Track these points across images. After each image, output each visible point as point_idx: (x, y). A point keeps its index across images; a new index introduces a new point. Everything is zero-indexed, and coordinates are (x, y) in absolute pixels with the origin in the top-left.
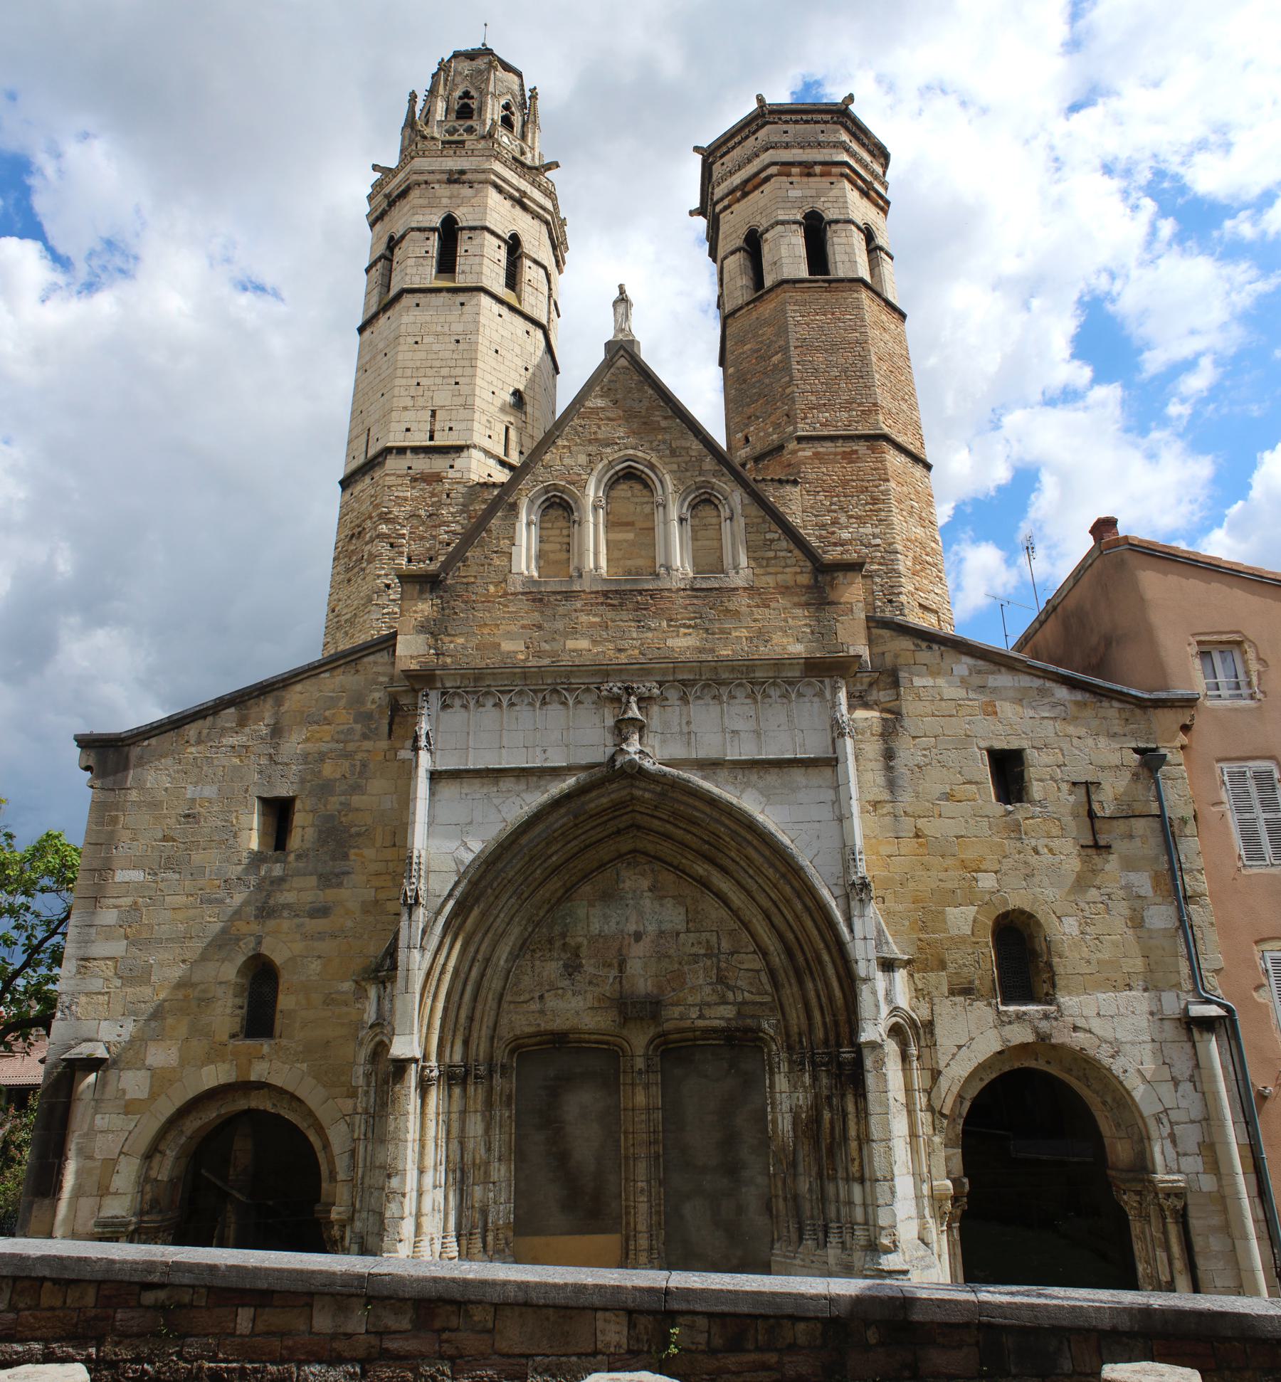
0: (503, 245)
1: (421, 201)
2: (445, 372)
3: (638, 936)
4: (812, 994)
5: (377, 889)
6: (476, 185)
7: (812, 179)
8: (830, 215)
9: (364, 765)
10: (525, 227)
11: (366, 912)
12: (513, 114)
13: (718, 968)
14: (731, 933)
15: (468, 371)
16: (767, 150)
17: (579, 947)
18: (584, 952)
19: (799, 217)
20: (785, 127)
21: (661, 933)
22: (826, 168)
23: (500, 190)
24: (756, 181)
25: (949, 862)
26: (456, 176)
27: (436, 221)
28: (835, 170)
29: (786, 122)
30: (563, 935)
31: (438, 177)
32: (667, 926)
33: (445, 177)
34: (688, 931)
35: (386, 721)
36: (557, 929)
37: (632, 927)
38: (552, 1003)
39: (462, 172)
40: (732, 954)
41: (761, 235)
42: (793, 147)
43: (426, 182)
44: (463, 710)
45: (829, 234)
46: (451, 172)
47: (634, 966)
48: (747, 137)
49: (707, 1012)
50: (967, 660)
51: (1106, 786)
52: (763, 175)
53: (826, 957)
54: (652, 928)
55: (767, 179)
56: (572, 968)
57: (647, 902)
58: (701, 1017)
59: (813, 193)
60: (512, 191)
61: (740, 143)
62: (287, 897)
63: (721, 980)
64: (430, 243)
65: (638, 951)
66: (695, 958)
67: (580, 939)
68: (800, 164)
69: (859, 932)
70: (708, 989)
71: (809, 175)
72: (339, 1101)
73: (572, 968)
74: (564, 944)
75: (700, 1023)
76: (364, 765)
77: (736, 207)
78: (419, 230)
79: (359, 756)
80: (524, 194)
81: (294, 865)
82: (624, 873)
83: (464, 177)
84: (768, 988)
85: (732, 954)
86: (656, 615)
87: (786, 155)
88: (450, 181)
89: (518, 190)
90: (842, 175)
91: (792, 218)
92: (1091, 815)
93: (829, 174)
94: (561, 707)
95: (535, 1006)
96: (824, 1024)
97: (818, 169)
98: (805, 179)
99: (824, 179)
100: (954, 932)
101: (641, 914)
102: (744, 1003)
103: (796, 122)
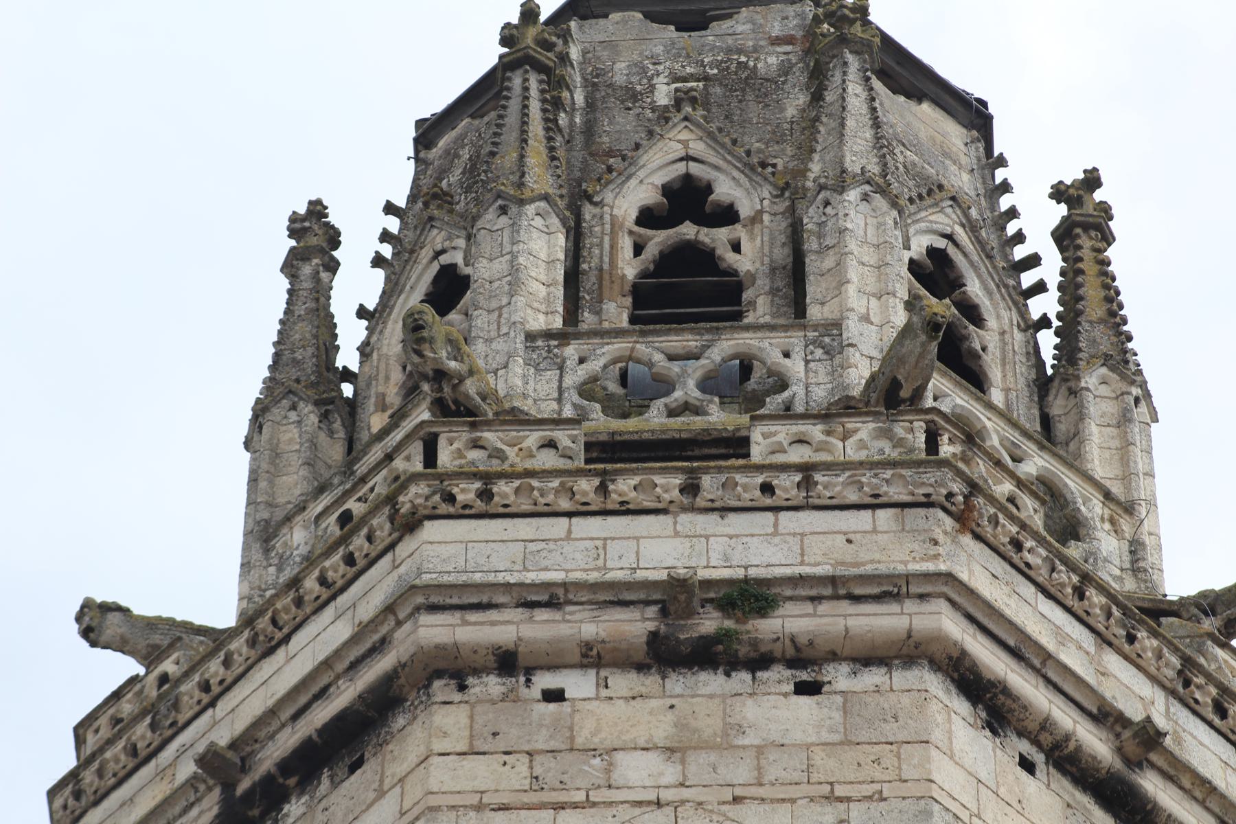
1: (481, 774)
6: (839, 677)
23: (995, 708)
26: (709, 623)
31: (587, 625)
33: (634, 626)
39: (750, 596)
43: (507, 662)
46: (675, 596)
60: (1066, 718)
80: (1146, 741)
83: (767, 627)
88: (666, 656)
89: (1105, 716)
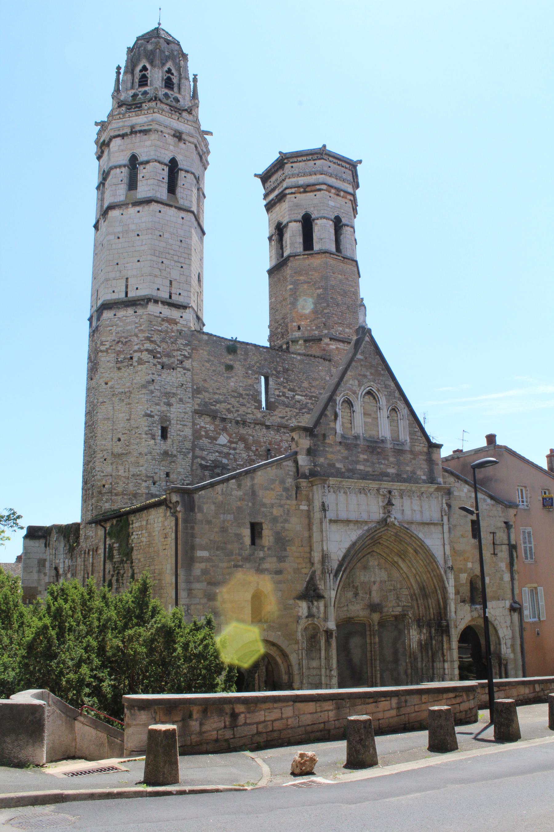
2: (176, 258)
3: (374, 583)
4: (430, 603)
5: (298, 564)
9: (288, 511)
11: (294, 573)
13: (397, 595)
14: (400, 582)
15: (187, 261)
16: (322, 174)
17: (357, 587)
18: (359, 588)
19: (333, 217)
20: (330, 164)
21: (381, 582)
22: (345, 194)
24: (313, 188)
25: (462, 558)
27: (167, 160)
29: (330, 161)
30: (353, 582)
32: (382, 579)
33: (173, 132)
34: (388, 581)
35: (294, 492)
36: (351, 579)
37: (373, 579)
38: (351, 607)
40: (400, 589)
41: (314, 220)
42: (333, 177)
43: (161, 132)
44: (334, 494)
47: (374, 594)
48: (310, 160)
49: (394, 609)
50: (467, 486)
51: (497, 534)
52: (318, 187)
53: (439, 592)
54: (378, 579)
55: (320, 190)
56: (356, 595)
57: (377, 570)
58: (393, 611)
61: (305, 161)
62: (266, 566)
63: (398, 598)
65: (375, 588)
66: (391, 591)
67: (358, 584)
68: (335, 188)
69: (450, 585)
70: (394, 602)
71: (338, 195)
72: (293, 645)
73: (356, 595)
74: (353, 586)
75: (393, 613)
76: (288, 511)
77: (298, 195)
78: (159, 162)
79: (286, 507)
81: (267, 552)
82: (370, 559)
84: (410, 601)
85: (400, 589)
86: (384, 459)
87: (332, 181)
92: (494, 544)
93: (346, 198)
94: (364, 496)
95: (345, 609)
96: (434, 613)
97: (342, 194)
98: (336, 197)
99: (343, 199)
100: (462, 582)
101: (375, 574)
102: (404, 606)
103: (335, 163)
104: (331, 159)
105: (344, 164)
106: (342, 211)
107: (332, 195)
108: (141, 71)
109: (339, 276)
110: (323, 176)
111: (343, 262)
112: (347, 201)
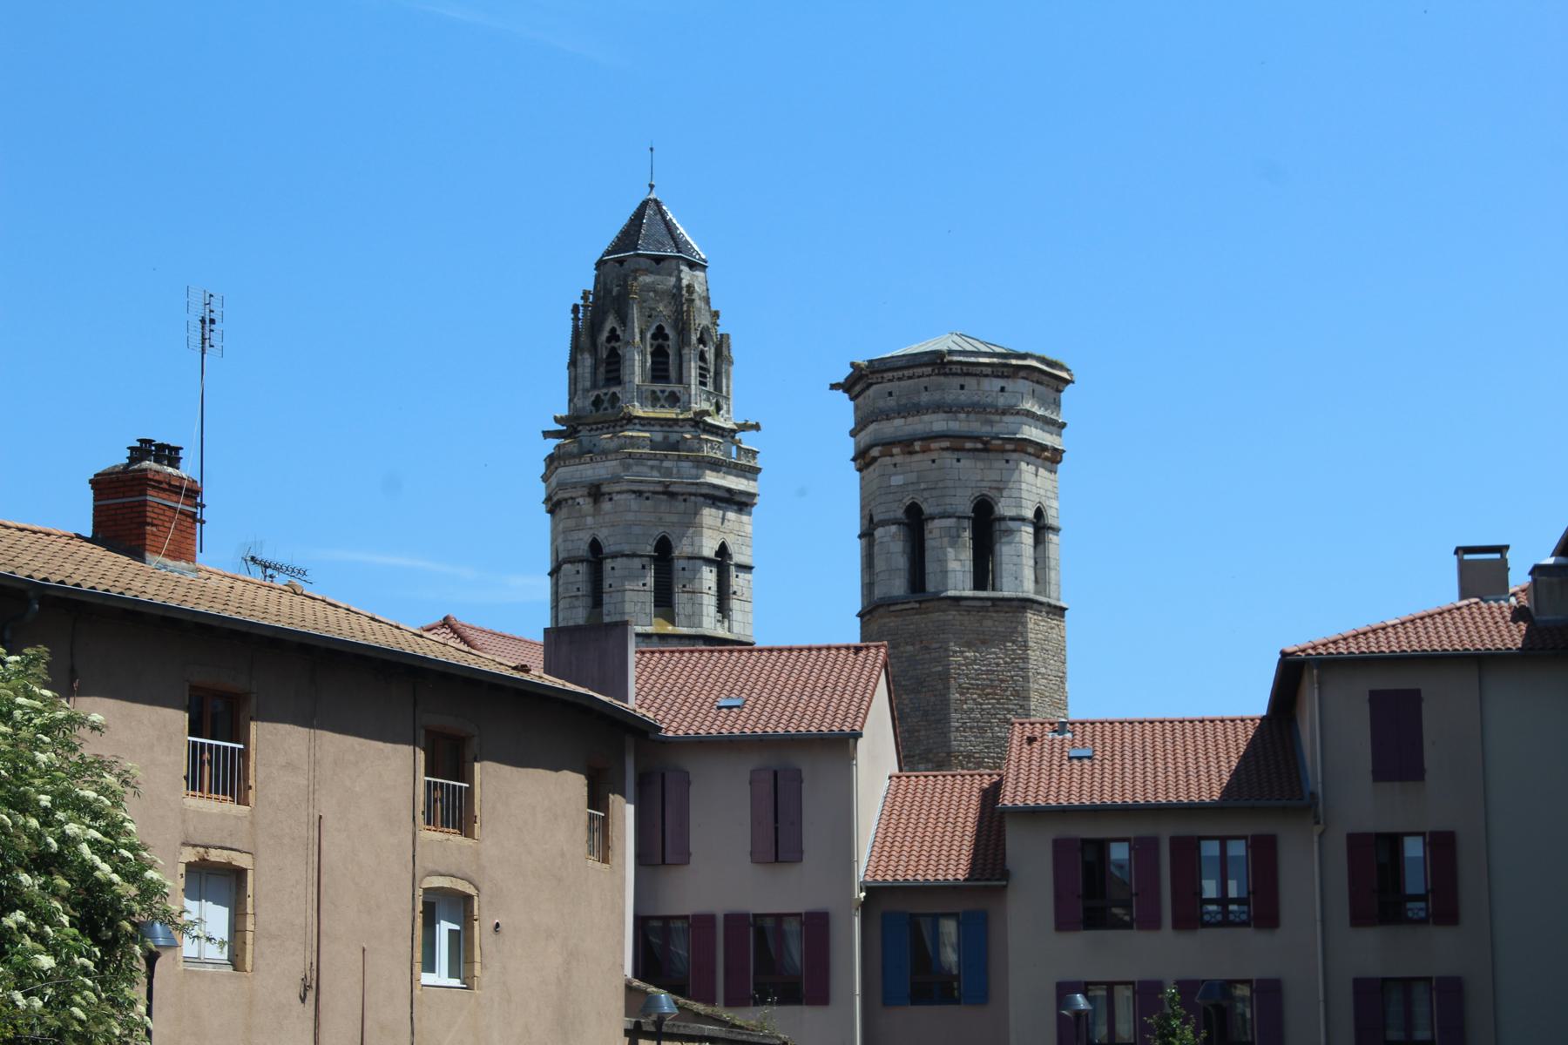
0: (646, 561)
6: (616, 497)
7: (916, 457)
8: (927, 509)
10: (674, 518)
12: (666, 337)
19: (900, 514)
20: (888, 386)
23: (639, 493)
28: (934, 445)
45: (927, 536)
59: (913, 477)
64: (579, 578)
71: (911, 453)
90: (943, 449)
91: (891, 515)
98: (908, 459)
104: (889, 375)
105: (919, 371)
106: (923, 486)
107: (898, 459)
108: (609, 340)
109: (910, 648)
110: (872, 427)
111: (918, 611)
112: (934, 455)
